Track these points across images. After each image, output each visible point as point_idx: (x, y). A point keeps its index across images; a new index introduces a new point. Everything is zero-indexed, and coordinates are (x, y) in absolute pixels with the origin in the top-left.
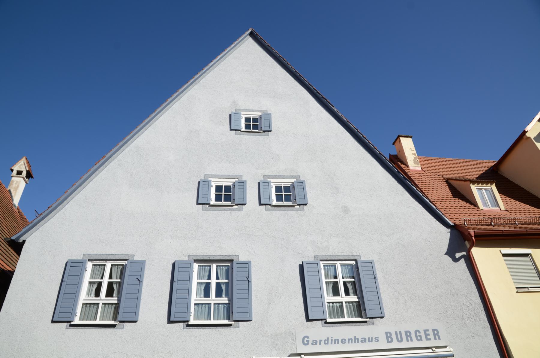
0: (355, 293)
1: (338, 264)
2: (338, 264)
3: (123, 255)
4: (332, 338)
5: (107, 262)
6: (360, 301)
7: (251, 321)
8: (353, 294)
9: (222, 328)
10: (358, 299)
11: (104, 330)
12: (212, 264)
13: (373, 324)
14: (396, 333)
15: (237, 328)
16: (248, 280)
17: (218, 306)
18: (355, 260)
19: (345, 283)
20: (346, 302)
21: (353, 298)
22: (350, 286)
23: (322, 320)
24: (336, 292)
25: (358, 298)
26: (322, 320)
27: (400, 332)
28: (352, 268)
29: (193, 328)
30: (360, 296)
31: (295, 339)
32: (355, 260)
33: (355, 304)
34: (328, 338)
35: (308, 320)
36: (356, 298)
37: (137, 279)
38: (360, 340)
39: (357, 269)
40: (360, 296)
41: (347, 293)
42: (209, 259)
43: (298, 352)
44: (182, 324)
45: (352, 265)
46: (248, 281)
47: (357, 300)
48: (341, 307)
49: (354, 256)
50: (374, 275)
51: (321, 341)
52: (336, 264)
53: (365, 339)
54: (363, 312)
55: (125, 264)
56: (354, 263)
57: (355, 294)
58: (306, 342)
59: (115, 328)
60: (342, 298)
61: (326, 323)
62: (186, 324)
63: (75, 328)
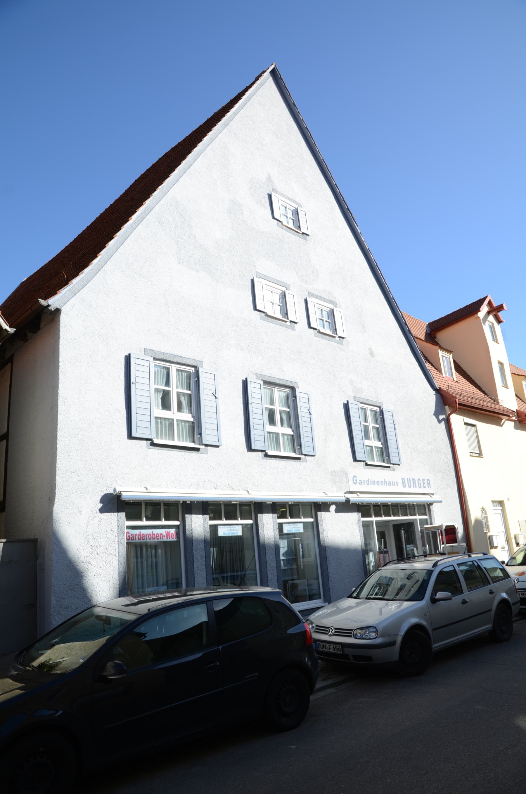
0: (290, 426)
1: (368, 408)
2: (173, 368)
3: (190, 360)
4: (371, 479)
5: (172, 365)
6: (195, 422)
7: (314, 456)
8: (286, 426)
9: (182, 452)
10: (193, 418)
11: (188, 453)
12: (274, 388)
13: (394, 470)
14: (407, 479)
15: (305, 462)
16: (310, 413)
17: (269, 435)
18: (380, 407)
19: (178, 394)
20: (177, 420)
21: (188, 417)
22: (284, 416)
23: (147, 439)
24: (166, 404)
25: (193, 417)
26: (147, 439)
27: (410, 479)
28: (189, 377)
29: (271, 458)
30: (294, 430)
31: (347, 478)
32: (195, 367)
33: (379, 449)
34: (369, 479)
35: (130, 436)
36: (191, 417)
37: (212, 395)
38: (388, 483)
39: (196, 379)
40: (294, 430)
41: (180, 408)
42: (274, 381)
43: (351, 490)
44: (260, 453)
45: (190, 372)
46: (309, 414)
47: (192, 420)
48: (372, 450)
49: (379, 403)
50: (394, 425)
51: (364, 481)
52: (171, 367)
53: (385, 482)
54: (197, 436)
55: (191, 371)
56: (192, 370)
57: (289, 427)
58: (355, 482)
59: (199, 452)
60: (173, 414)
61: (266, 455)
62: (264, 454)
63: (157, 448)
